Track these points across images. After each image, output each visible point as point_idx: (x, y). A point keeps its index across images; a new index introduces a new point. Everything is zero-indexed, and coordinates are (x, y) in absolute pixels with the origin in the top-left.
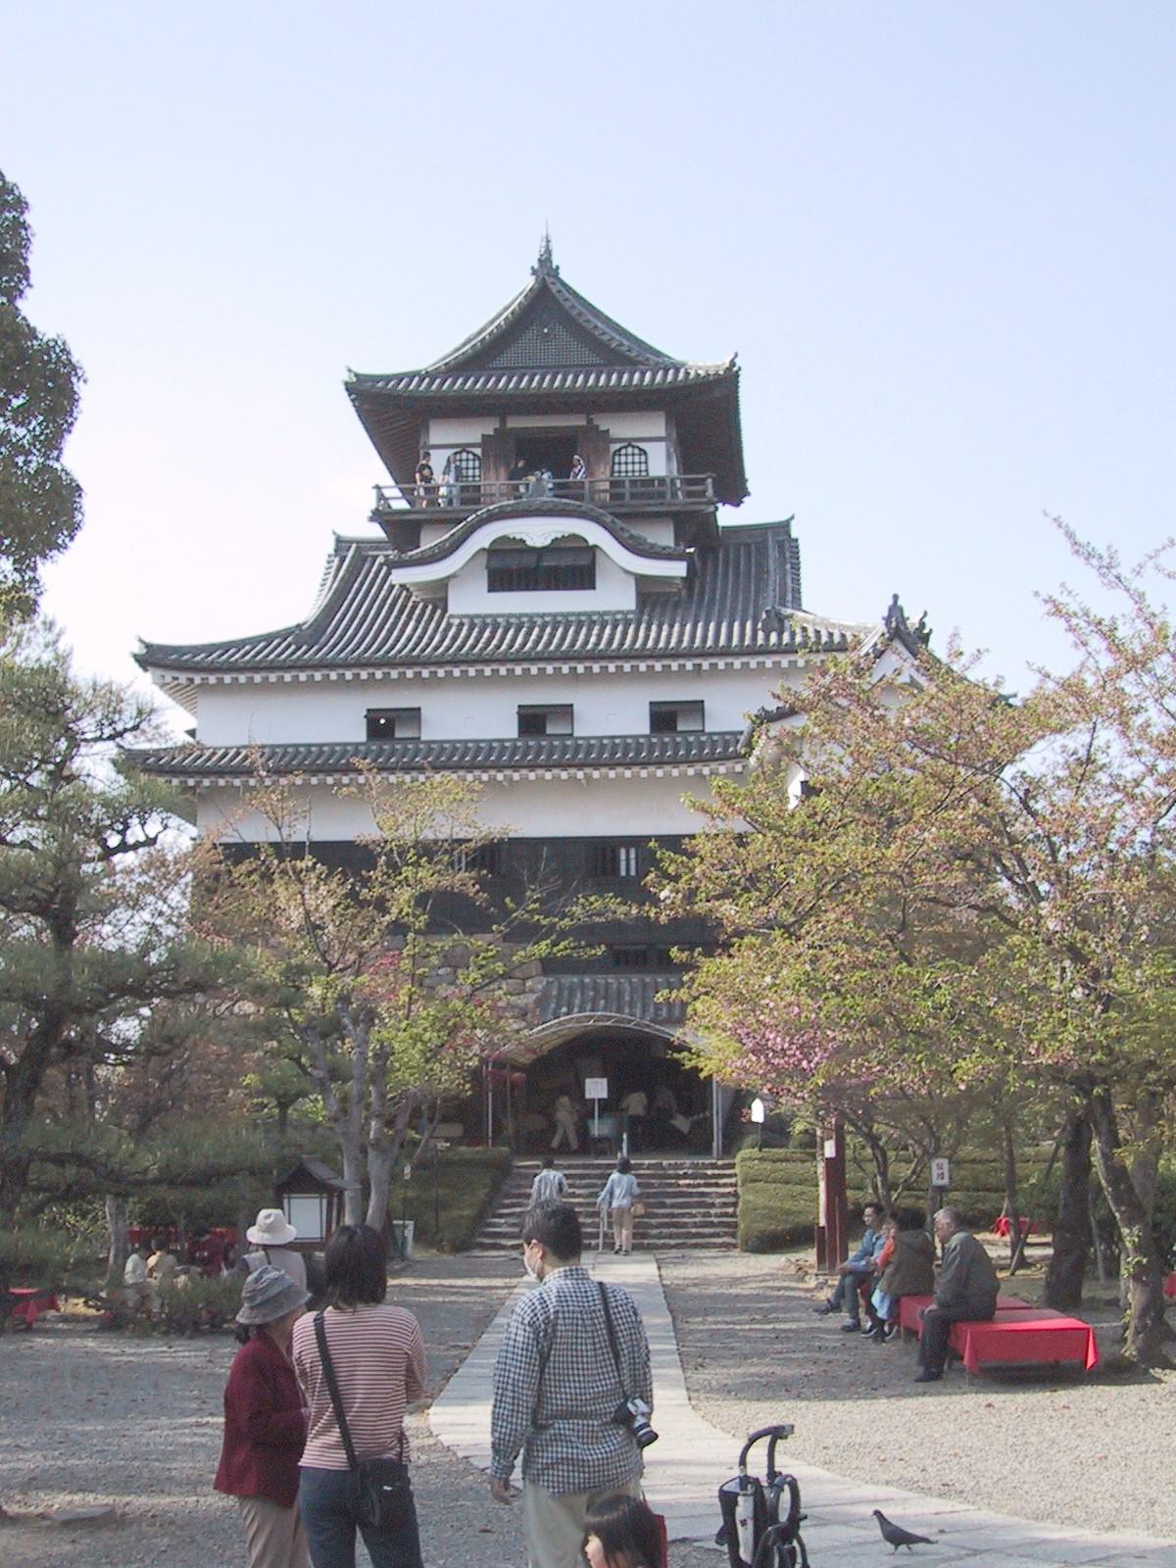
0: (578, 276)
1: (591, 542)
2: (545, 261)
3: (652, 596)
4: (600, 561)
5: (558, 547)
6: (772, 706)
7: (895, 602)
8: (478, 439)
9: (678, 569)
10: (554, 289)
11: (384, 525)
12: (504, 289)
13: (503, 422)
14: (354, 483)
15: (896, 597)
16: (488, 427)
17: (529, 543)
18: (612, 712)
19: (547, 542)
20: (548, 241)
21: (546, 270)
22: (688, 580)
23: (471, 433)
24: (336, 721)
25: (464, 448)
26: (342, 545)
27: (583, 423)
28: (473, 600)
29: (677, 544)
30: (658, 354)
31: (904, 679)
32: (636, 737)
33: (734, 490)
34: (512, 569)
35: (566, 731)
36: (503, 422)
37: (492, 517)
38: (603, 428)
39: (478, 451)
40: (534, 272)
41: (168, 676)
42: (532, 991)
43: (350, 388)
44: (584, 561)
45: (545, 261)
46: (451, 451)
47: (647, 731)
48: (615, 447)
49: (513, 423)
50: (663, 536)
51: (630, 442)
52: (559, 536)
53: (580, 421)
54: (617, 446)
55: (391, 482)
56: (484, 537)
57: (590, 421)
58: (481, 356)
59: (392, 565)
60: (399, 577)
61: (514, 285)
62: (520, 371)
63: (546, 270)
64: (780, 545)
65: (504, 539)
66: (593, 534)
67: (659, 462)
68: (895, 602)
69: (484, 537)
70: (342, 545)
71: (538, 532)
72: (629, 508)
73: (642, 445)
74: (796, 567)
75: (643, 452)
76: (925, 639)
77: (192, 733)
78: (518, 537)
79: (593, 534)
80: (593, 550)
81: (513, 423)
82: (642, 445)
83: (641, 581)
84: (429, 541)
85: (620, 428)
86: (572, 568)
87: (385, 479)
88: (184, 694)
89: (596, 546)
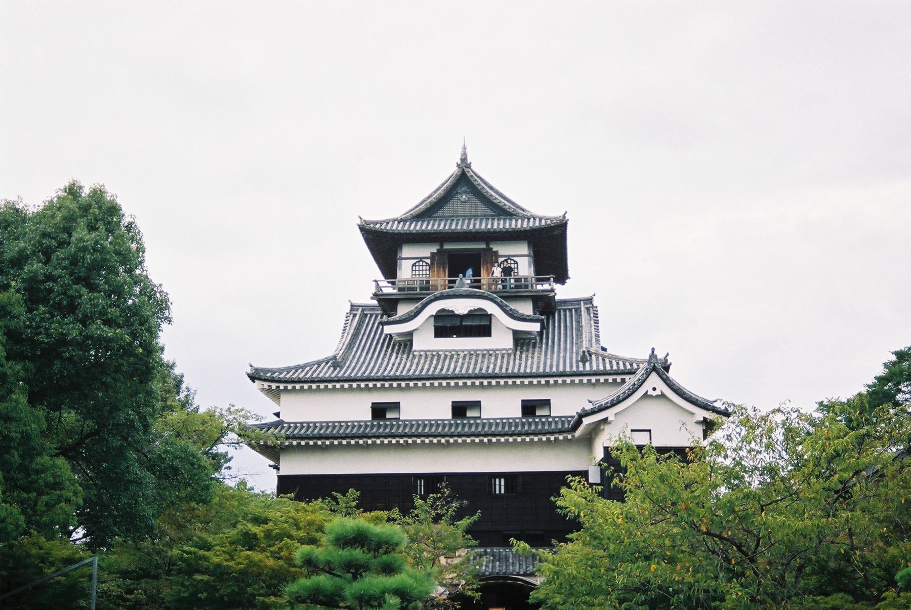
0: (481, 169)
1: (489, 313)
2: (464, 159)
3: (521, 340)
4: (493, 321)
5: (472, 315)
6: (589, 407)
7: (653, 352)
8: (429, 255)
9: (535, 327)
10: (470, 174)
11: (379, 301)
12: (441, 174)
13: (442, 246)
14: (364, 278)
15: (653, 349)
17: (456, 312)
18: (501, 406)
19: (466, 312)
20: (465, 148)
21: (464, 164)
22: (541, 334)
23: (426, 251)
24: (355, 409)
25: (421, 259)
26: (353, 307)
27: (484, 246)
28: (426, 341)
29: (535, 313)
30: (523, 210)
31: (658, 392)
32: (514, 419)
33: (562, 277)
34: (447, 326)
35: (477, 415)
36: (442, 246)
37: (437, 299)
38: (495, 249)
39: (429, 261)
40: (458, 165)
41: (266, 385)
42: (459, 556)
43: (362, 229)
44: (484, 323)
45: (464, 159)
46: (415, 261)
47: (520, 415)
49: (447, 246)
50: (526, 309)
51: (509, 257)
54: (503, 259)
55: (383, 278)
56: (433, 308)
57: (488, 245)
58: (429, 211)
59: (383, 324)
60: (388, 329)
61: (447, 171)
62: (452, 218)
63: (464, 164)
64: (588, 309)
65: (443, 310)
66: (490, 307)
67: (525, 268)
68: (653, 352)
69: (433, 308)
70: (353, 307)
71: (461, 307)
72: (507, 296)
74: (597, 322)
75: (516, 263)
76: (667, 368)
77: (277, 415)
79: (490, 307)
80: (489, 317)
81: (447, 246)
83: (516, 333)
84: (403, 310)
85: (504, 250)
86: (479, 326)
87: (379, 276)
88: (275, 394)
89: (491, 315)
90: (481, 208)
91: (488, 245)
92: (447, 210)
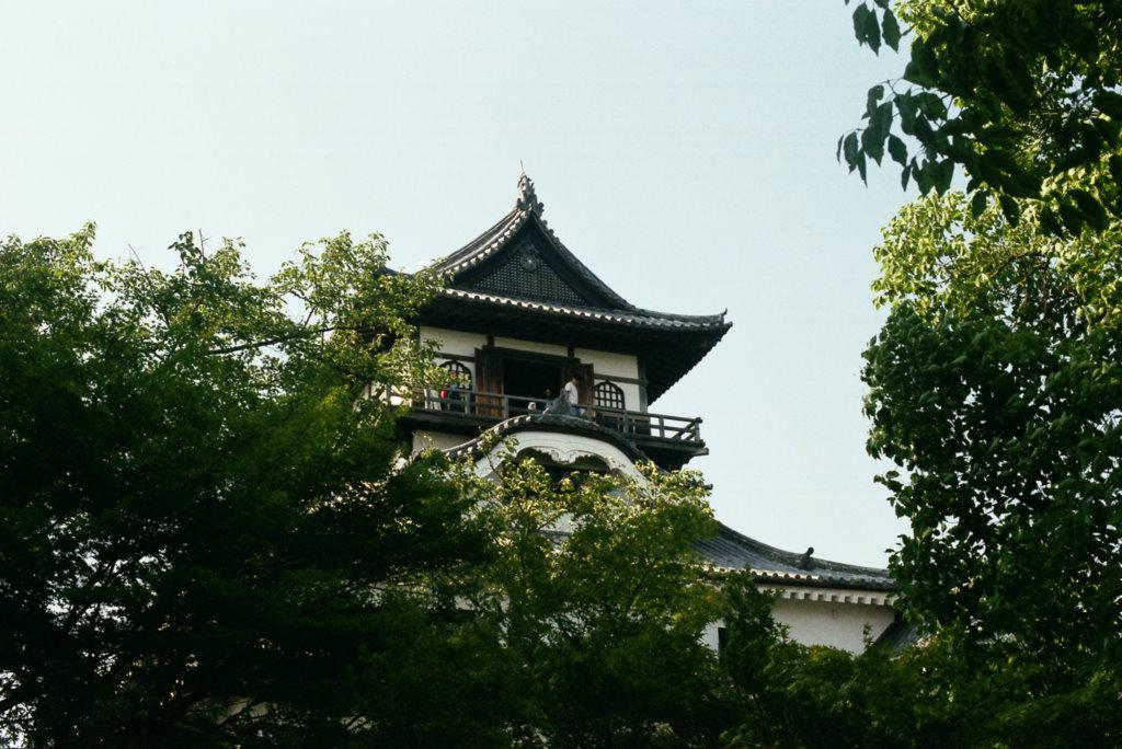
13: (491, 341)
16: (479, 342)
17: (554, 458)
21: (530, 203)
23: (464, 346)
27: (562, 352)
36: (491, 341)
48: (597, 382)
49: (501, 343)
51: (608, 380)
52: (583, 455)
53: (562, 352)
57: (571, 352)
61: (492, 209)
63: (530, 203)
66: (613, 456)
73: (619, 385)
75: (619, 391)
78: (544, 451)
81: (501, 343)
82: (619, 385)
90: (558, 287)
91: (571, 352)
92: (499, 278)
